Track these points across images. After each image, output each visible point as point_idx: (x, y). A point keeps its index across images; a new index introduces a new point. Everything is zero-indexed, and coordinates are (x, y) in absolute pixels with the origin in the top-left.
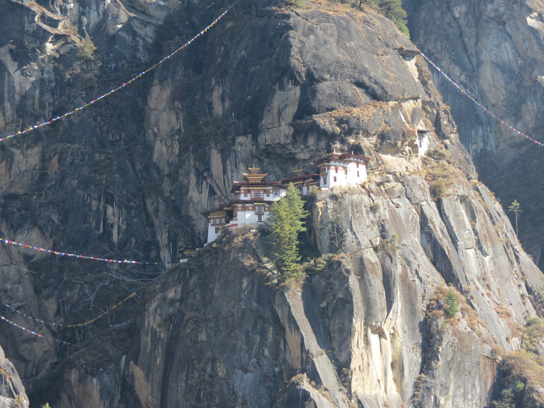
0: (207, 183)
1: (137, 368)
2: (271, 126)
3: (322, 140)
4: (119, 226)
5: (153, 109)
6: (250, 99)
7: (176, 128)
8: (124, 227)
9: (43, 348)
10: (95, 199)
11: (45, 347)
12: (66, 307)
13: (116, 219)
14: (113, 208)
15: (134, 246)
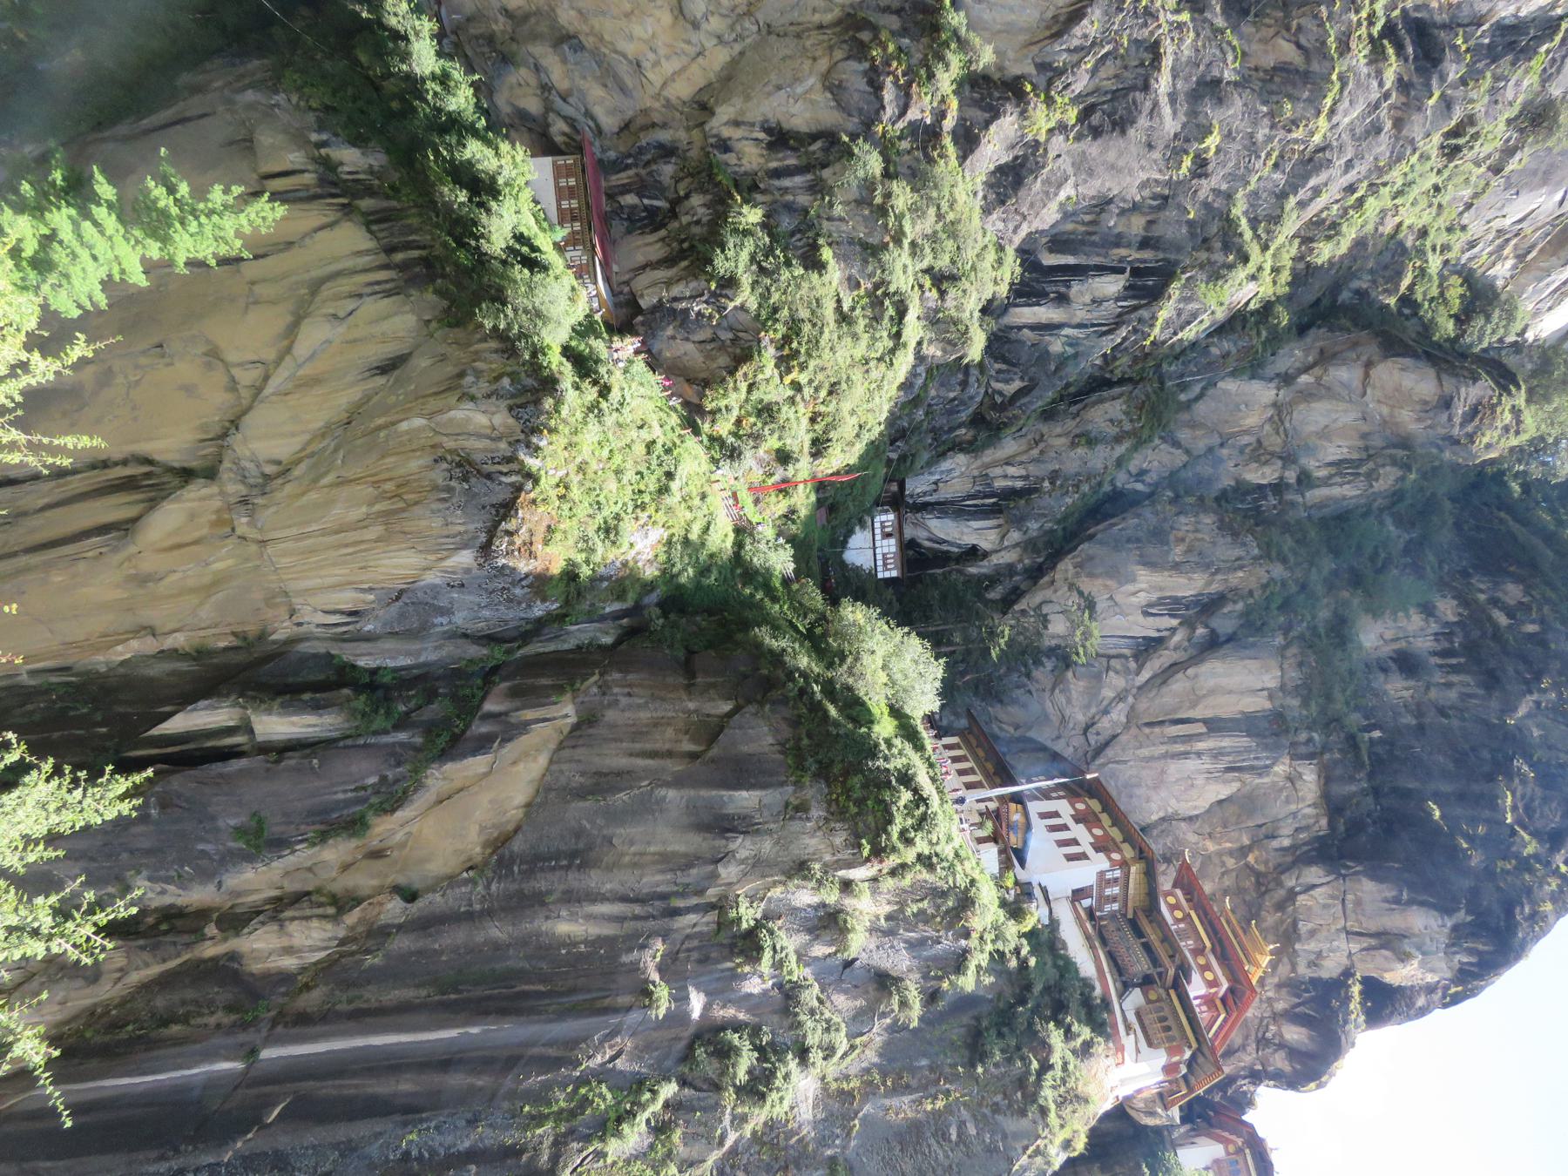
0: (1173, 630)
1: (543, 760)
2: (1350, 906)
3: (1290, 1061)
4: (1060, 326)
5: (1367, 375)
6: (1430, 814)
7: (1310, 463)
8: (1056, 346)
9: (651, 56)
10: (1150, 223)
11: (657, 64)
12: (798, 180)
13: (1081, 315)
14: (1117, 299)
15: (994, 391)
